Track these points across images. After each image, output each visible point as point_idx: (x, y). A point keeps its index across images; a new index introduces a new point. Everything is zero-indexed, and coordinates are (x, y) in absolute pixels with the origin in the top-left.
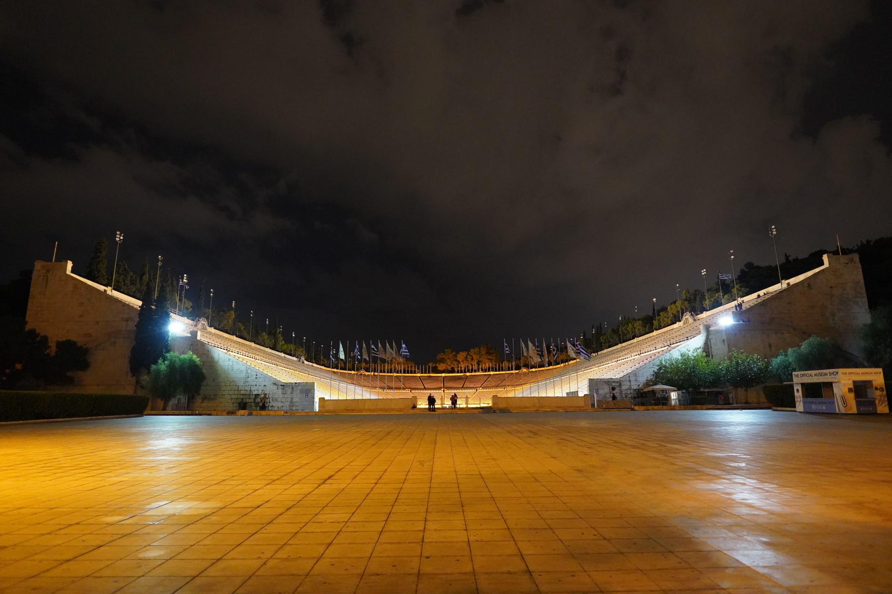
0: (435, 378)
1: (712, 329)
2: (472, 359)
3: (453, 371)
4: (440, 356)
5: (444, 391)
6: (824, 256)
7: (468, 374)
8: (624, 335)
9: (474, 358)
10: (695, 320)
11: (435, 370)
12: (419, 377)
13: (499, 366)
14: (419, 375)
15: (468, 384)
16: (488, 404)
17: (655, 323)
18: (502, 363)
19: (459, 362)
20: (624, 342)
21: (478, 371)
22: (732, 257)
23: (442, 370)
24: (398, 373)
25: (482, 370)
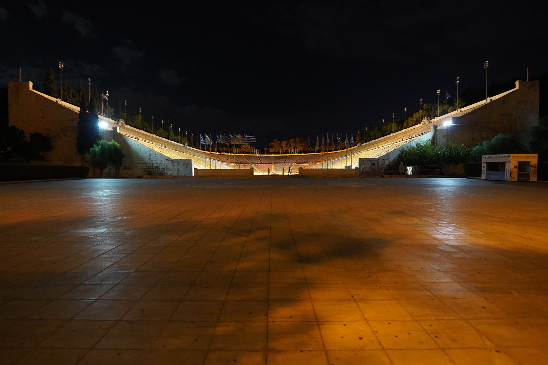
0: (268, 157)
1: (438, 128)
2: (290, 146)
3: (279, 153)
4: (271, 144)
5: (273, 165)
6: (516, 81)
7: (288, 155)
8: (385, 132)
9: (292, 145)
10: (429, 123)
11: (268, 153)
12: (258, 156)
13: (307, 150)
14: (258, 155)
15: (288, 161)
17: (405, 124)
20: (384, 136)
21: (294, 153)
22: (458, 82)
23: (272, 152)
25: (297, 152)
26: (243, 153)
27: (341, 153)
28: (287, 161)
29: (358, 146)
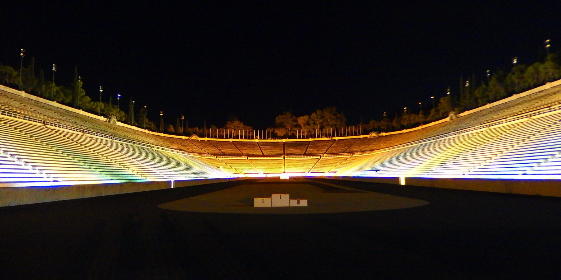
2: (314, 124)
3: (294, 137)
4: (278, 120)
5: (284, 158)
7: (311, 140)
8: (513, 84)
10: (457, 117)
11: (274, 136)
12: (258, 143)
13: (345, 131)
14: (257, 141)
15: (311, 150)
16: (335, 172)
18: (348, 128)
19: (300, 127)
24: (234, 138)
26: (230, 138)
27: (411, 134)
28: (310, 150)
29: (451, 119)
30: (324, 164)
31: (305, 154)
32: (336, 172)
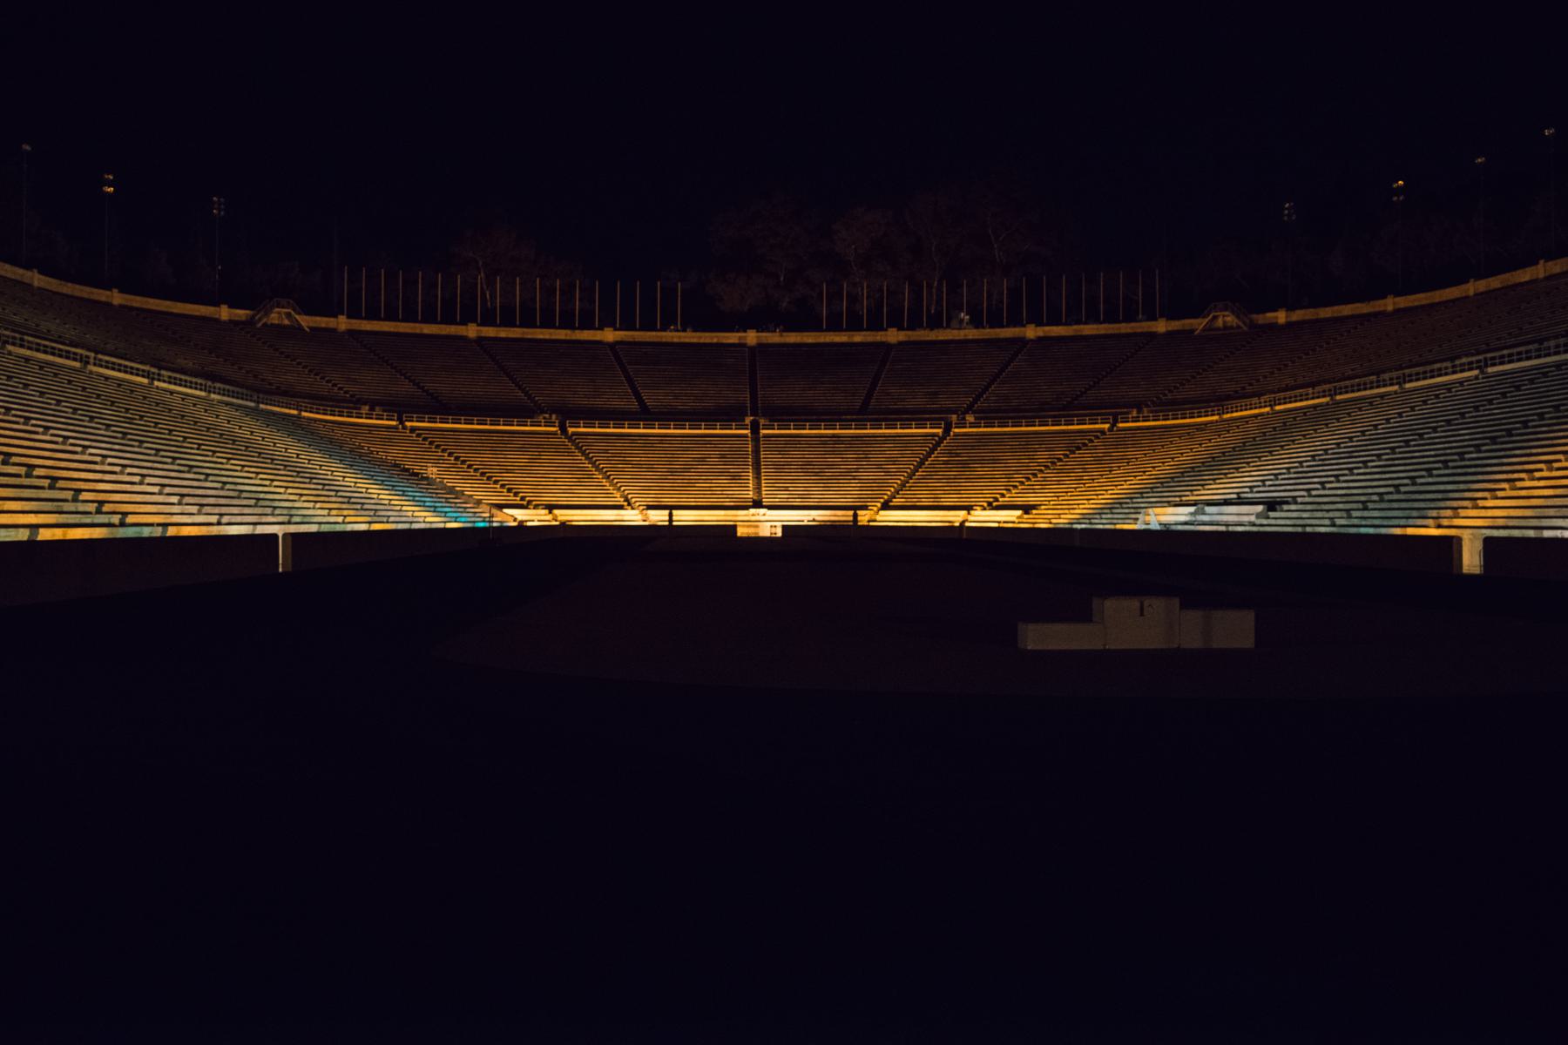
5: (755, 428)
7: (893, 336)
12: (613, 346)
14: (609, 335)
16: (1027, 509)
24: (485, 322)
30: (965, 465)
31: (864, 414)
32: (1034, 507)
